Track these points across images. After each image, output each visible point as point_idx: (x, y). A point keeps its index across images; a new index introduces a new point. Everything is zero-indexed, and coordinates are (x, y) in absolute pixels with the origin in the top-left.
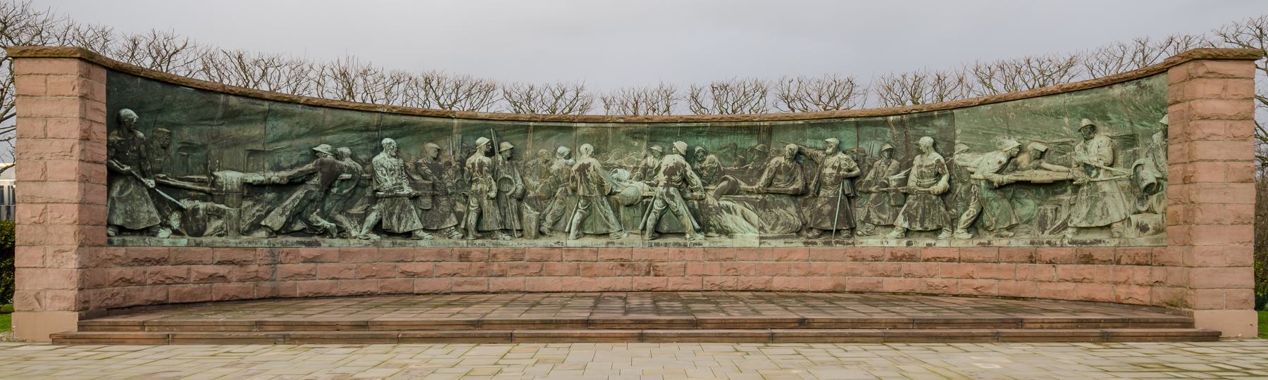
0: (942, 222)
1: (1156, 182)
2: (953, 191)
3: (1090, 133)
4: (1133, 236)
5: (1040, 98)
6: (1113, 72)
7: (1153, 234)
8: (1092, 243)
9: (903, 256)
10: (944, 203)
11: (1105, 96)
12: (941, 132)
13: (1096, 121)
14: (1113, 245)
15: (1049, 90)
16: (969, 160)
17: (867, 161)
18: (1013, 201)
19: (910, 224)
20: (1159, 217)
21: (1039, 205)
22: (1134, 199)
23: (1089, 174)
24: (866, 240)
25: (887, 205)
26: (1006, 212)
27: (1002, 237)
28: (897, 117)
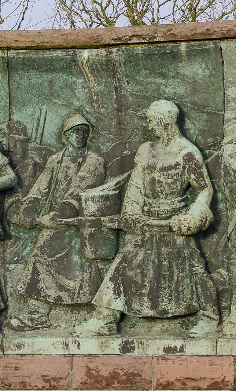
0: (198, 297)
2: (221, 228)
9: (114, 376)
10: (203, 255)
12: (195, 91)
17: (32, 154)
19: (128, 303)
24: (29, 340)
25: (76, 258)
28: (99, 51)
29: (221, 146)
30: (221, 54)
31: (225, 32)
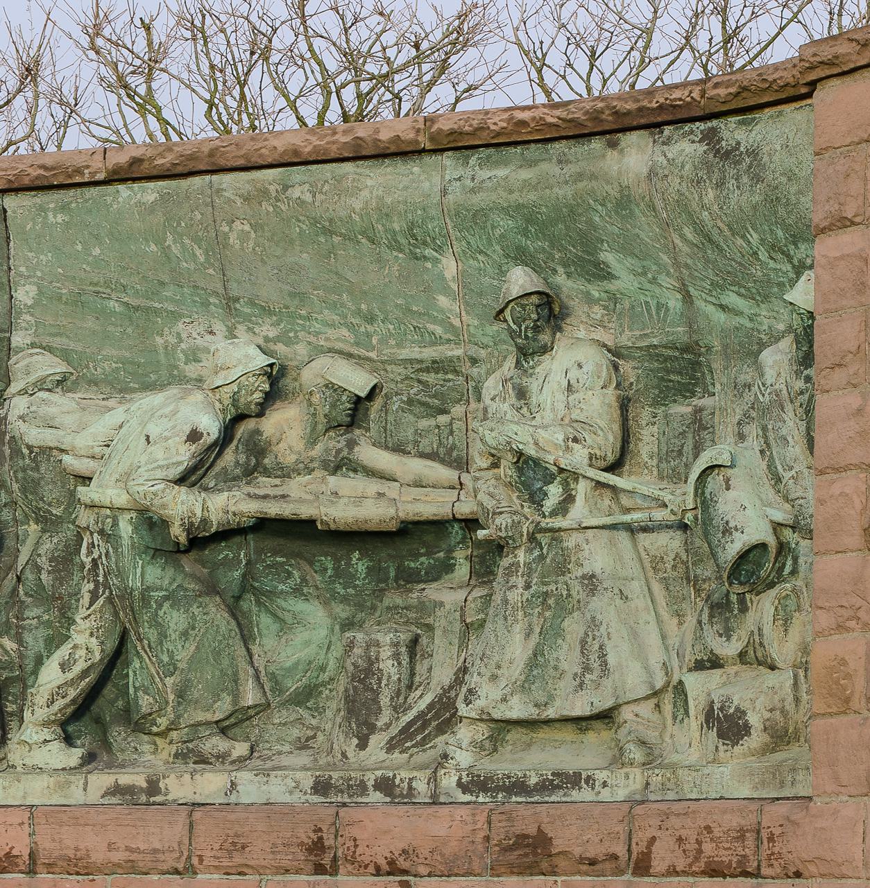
1: (771, 541)
3: (537, 329)
4: (693, 756)
5: (348, 167)
6: (614, 87)
7: (766, 750)
8: (546, 786)
11: (593, 177)
13: (560, 279)
14: (621, 794)
15: (385, 136)
16: (69, 420)
18: (244, 605)
20: (782, 680)
21: (348, 625)
22: (694, 609)
23: (536, 499)
26: (217, 654)
27: (202, 760)
29: (5, 400)
30: (5, 220)
31: (13, 179)
